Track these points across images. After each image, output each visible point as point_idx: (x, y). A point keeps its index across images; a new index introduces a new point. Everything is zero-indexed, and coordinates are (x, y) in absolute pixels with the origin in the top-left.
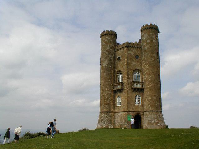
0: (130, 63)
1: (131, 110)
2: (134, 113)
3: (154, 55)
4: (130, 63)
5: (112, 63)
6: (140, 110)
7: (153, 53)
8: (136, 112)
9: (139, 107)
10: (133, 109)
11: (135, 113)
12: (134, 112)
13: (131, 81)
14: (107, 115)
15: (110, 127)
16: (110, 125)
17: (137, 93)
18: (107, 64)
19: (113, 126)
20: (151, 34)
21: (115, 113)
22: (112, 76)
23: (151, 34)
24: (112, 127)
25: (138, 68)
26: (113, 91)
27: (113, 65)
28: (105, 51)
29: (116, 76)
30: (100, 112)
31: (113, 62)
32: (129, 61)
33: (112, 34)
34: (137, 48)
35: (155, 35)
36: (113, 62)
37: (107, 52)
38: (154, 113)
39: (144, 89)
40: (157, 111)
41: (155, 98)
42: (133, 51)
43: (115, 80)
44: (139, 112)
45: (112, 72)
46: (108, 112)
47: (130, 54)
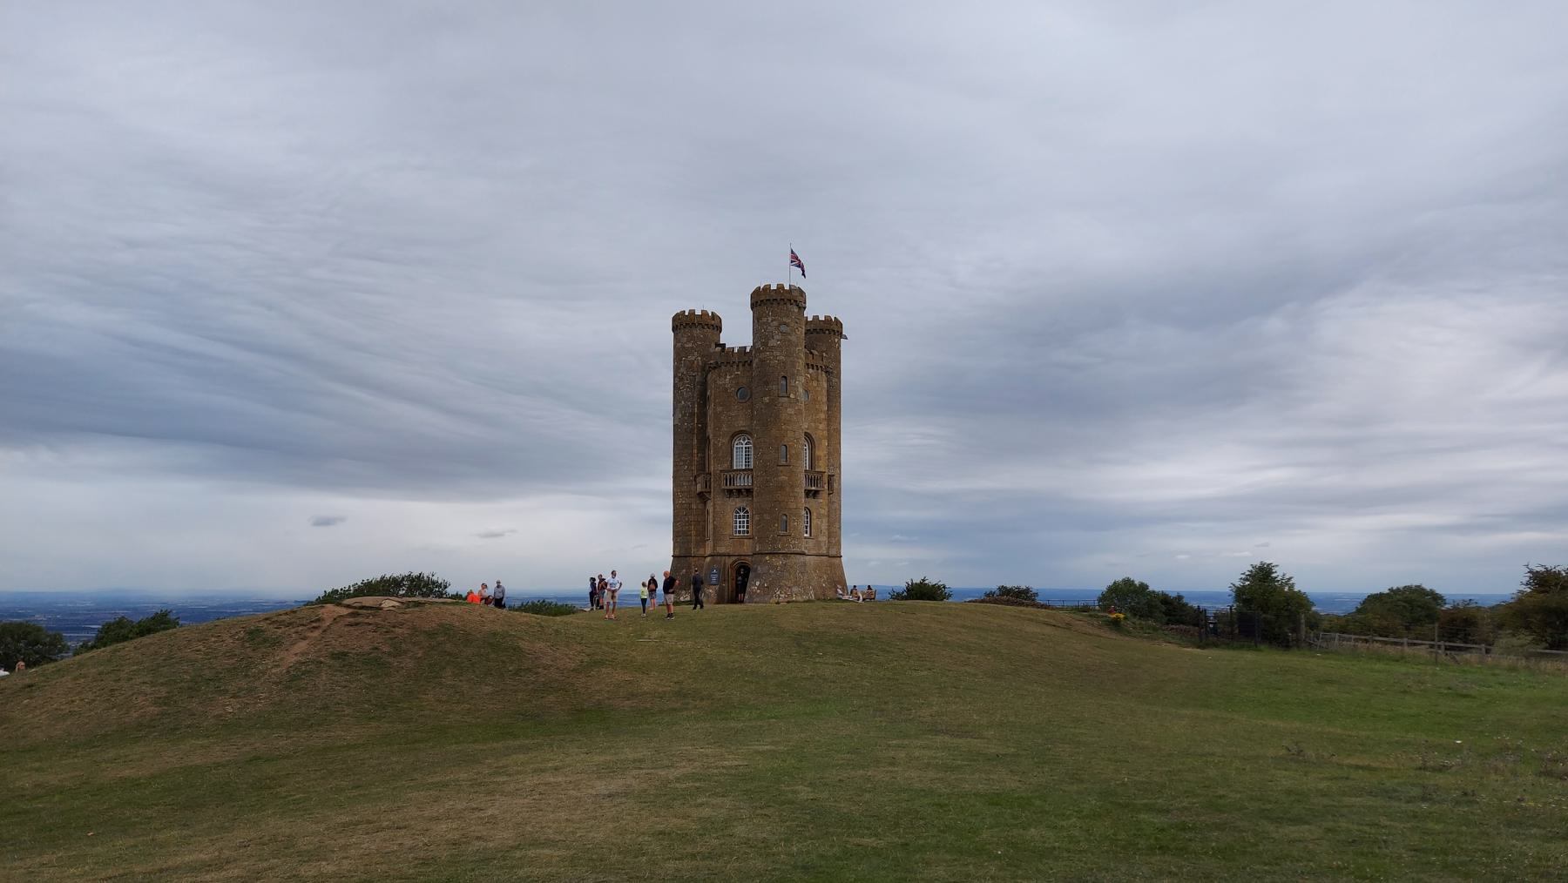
1: (721, 550)
2: (729, 561)
5: (692, 414)
6: (747, 548)
9: (746, 540)
11: (734, 558)
12: (729, 556)
13: (725, 466)
16: (684, 592)
17: (739, 502)
22: (695, 451)
25: (741, 424)
26: (698, 494)
28: (677, 379)
29: (707, 450)
32: (719, 409)
34: (744, 365)
35: (775, 323)
43: (704, 465)
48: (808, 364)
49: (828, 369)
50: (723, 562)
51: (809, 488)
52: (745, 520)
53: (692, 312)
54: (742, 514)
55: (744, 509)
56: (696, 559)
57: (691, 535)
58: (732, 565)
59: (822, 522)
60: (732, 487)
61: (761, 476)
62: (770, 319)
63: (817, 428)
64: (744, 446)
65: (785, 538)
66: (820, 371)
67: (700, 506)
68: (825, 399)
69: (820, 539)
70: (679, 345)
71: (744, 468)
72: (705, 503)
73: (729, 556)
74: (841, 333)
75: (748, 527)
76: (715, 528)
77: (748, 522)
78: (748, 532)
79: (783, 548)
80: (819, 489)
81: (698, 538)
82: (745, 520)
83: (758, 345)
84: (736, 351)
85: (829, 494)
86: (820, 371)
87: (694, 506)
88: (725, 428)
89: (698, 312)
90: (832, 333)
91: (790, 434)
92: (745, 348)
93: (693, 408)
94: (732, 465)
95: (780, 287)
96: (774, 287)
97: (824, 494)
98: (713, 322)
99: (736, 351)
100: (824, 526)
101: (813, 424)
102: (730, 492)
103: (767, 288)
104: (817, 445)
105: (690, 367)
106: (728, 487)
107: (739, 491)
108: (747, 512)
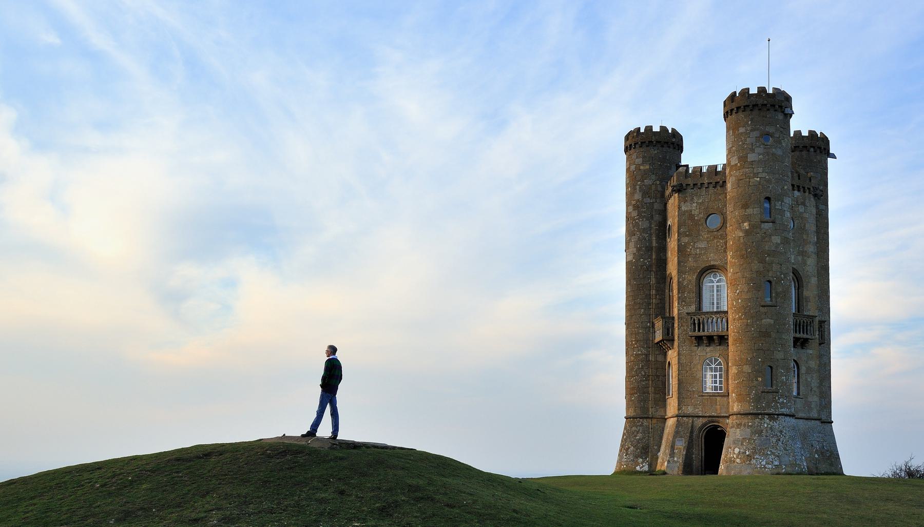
0: (686, 246)
1: (690, 410)
2: (699, 422)
3: (749, 211)
4: (686, 246)
5: (649, 249)
7: (745, 206)
8: (706, 417)
9: (718, 398)
10: (695, 406)
11: (704, 420)
12: (699, 417)
13: (692, 308)
14: (634, 428)
15: (638, 468)
16: (640, 460)
18: (634, 254)
19: (650, 465)
20: (742, 130)
21: (666, 419)
22: (654, 292)
23: (742, 130)
24: (646, 468)
27: (654, 257)
28: (631, 208)
30: (625, 418)
31: (654, 244)
32: (686, 240)
33: (651, 142)
34: (715, 187)
36: (654, 244)
37: (634, 210)
38: (745, 420)
39: (728, 335)
40: (756, 415)
41: (747, 369)
42: (700, 201)
43: (664, 308)
44: (718, 417)
45: (653, 281)
46: (640, 418)
47: (691, 217)
48: (793, 185)
49: (818, 192)
50: (690, 425)
51: (798, 335)
52: (718, 373)
53: (649, 129)
54: (713, 366)
55: (716, 360)
56: (654, 421)
57: (648, 393)
58: (701, 428)
59: (812, 377)
60: (701, 333)
61: (740, 318)
62: (749, 128)
63: (805, 263)
64: (715, 284)
65: (770, 396)
66: (807, 194)
67: (660, 358)
68: (814, 228)
69: (810, 399)
70: (633, 167)
71: (715, 310)
72: (665, 355)
73: (699, 417)
74: (829, 151)
75: (721, 382)
76: (680, 383)
77: (721, 376)
78: (721, 388)
79: (768, 406)
80: (810, 337)
81: (657, 396)
82: (718, 373)
83: (735, 161)
84: (704, 170)
85: (820, 344)
86: (807, 194)
87: (651, 358)
88: (691, 262)
89: (656, 129)
90: (818, 151)
91: (775, 267)
92: (716, 166)
93: (650, 241)
94: (699, 307)
95: (762, 90)
96: (754, 91)
97: (814, 344)
98: (674, 140)
99: (704, 170)
100: (815, 384)
101: (800, 258)
102: (699, 339)
103: (745, 92)
104: (805, 284)
105: (645, 193)
106: (697, 333)
107: (710, 339)
108: (720, 364)
